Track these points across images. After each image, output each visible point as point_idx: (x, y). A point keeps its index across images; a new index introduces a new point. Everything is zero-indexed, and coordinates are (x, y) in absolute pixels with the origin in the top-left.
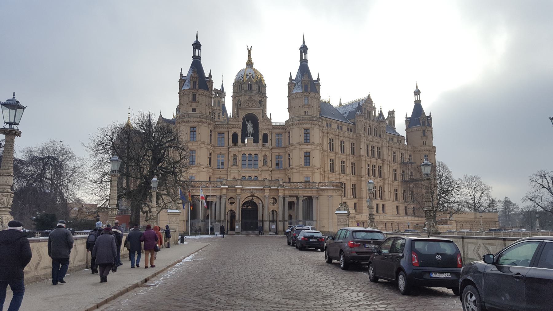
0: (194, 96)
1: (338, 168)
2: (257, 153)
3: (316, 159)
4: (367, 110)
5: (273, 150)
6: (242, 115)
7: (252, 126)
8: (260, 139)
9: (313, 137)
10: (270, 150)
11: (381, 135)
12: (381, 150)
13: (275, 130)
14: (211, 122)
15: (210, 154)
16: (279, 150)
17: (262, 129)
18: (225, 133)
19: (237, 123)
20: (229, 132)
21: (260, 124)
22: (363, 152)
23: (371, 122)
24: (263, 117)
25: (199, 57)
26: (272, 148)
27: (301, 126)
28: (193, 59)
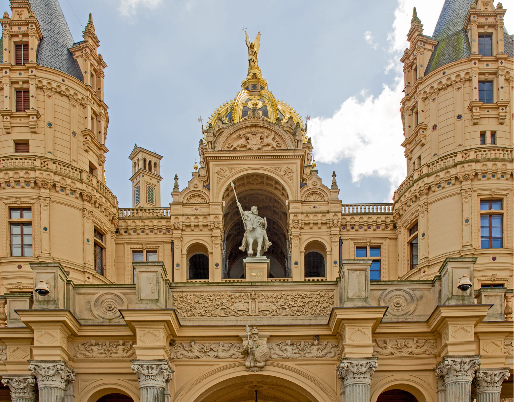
17: (301, 228)
21: (293, 208)
24: (303, 185)
27: (467, 184)
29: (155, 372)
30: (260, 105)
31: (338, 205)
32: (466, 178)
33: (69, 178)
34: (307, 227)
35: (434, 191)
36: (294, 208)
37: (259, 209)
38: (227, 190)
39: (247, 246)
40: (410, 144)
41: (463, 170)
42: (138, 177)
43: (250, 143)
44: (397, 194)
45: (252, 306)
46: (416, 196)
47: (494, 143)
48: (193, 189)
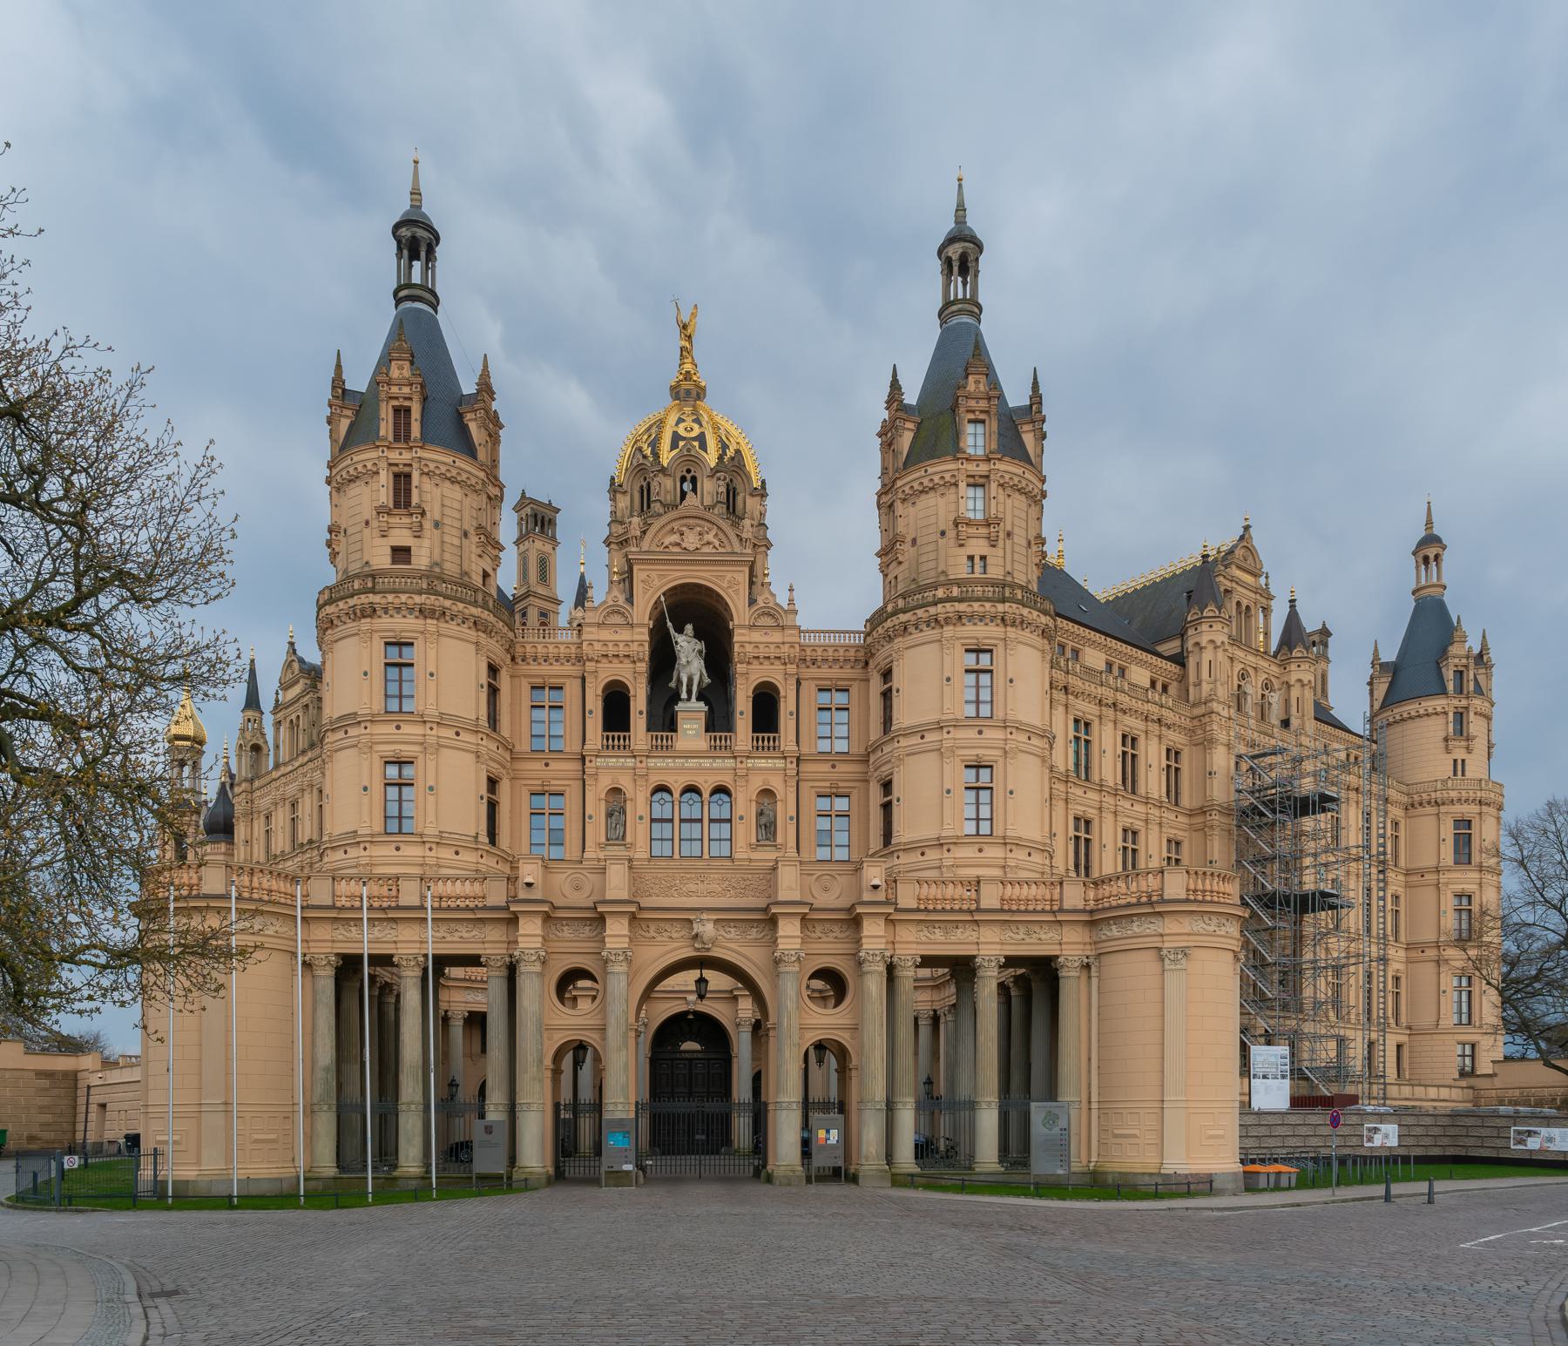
2: (728, 780)
4: (1236, 598)
5: (804, 767)
6: (652, 586)
7: (700, 652)
8: (742, 713)
9: (1010, 690)
10: (789, 766)
13: (813, 671)
14: (491, 618)
17: (749, 663)
18: (567, 689)
19: (625, 635)
20: (583, 679)
24: (752, 602)
26: (798, 759)
27: (948, 631)
29: (621, 958)
30: (696, 431)
31: (795, 632)
32: (947, 621)
33: (462, 602)
34: (755, 662)
35: (911, 634)
36: (743, 635)
37: (695, 629)
38: (656, 603)
39: (679, 681)
40: (886, 554)
41: (943, 610)
42: (526, 543)
43: (686, 540)
44: (868, 624)
45: (701, 887)
46: (889, 636)
47: (985, 573)
48: (612, 603)
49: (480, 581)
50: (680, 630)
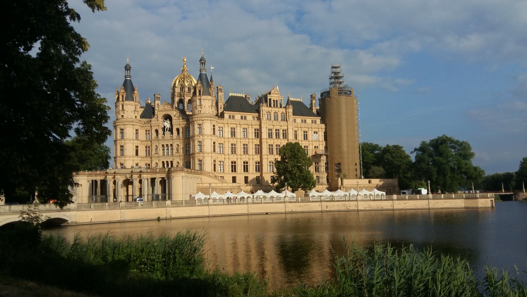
0: (123, 105)
1: (240, 150)
2: (172, 143)
3: (208, 146)
11: (288, 119)
12: (287, 132)
14: (136, 124)
15: (137, 147)
16: (188, 140)
19: (157, 122)
21: (173, 121)
22: (265, 135)
23: (276, 110)
24: (175, 116)
25: (130, 77)
28: (125, 78)
49: (135, 117)
50: (167, 120)
